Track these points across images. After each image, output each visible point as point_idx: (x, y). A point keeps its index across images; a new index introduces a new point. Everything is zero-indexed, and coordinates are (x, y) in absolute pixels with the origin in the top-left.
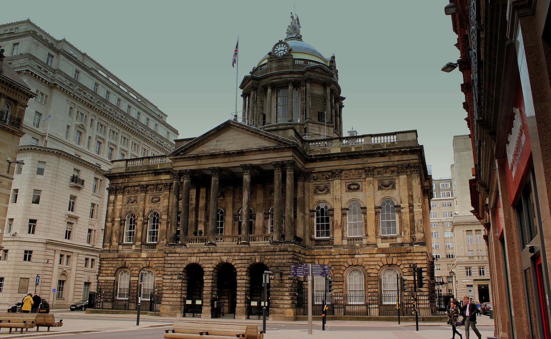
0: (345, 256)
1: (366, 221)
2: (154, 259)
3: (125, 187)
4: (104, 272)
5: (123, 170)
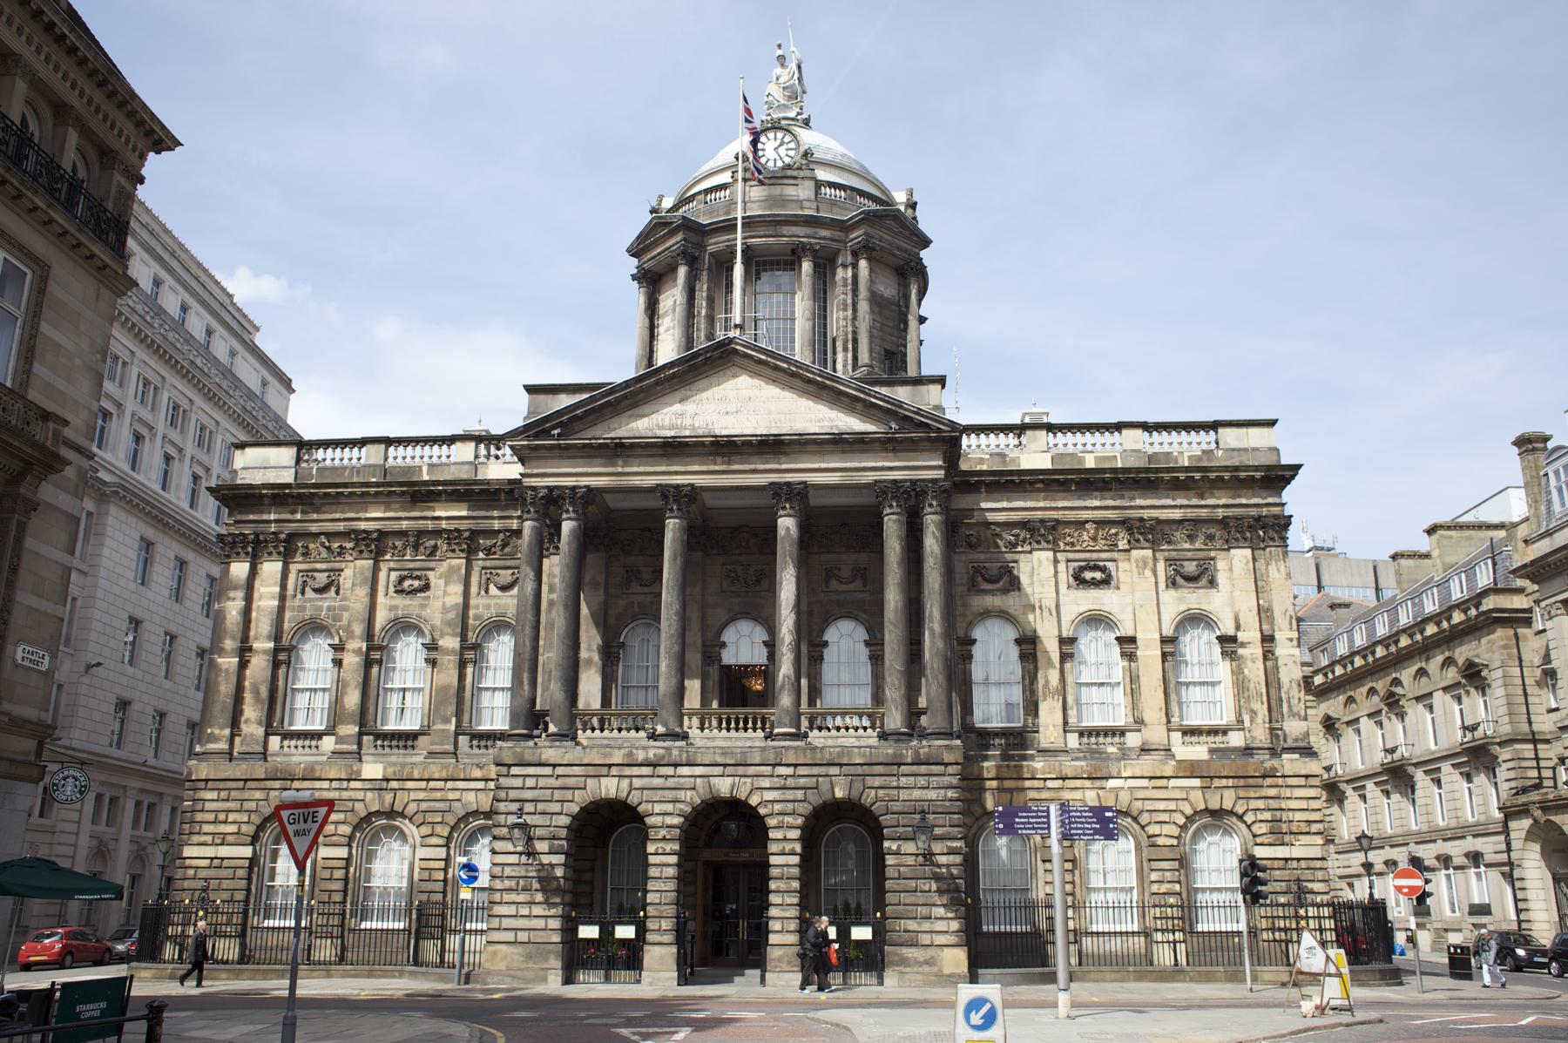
0: (1078, 783)
2: (410, 785)
3: (293, 536)
4: (207, 828)
5: (287, 477)
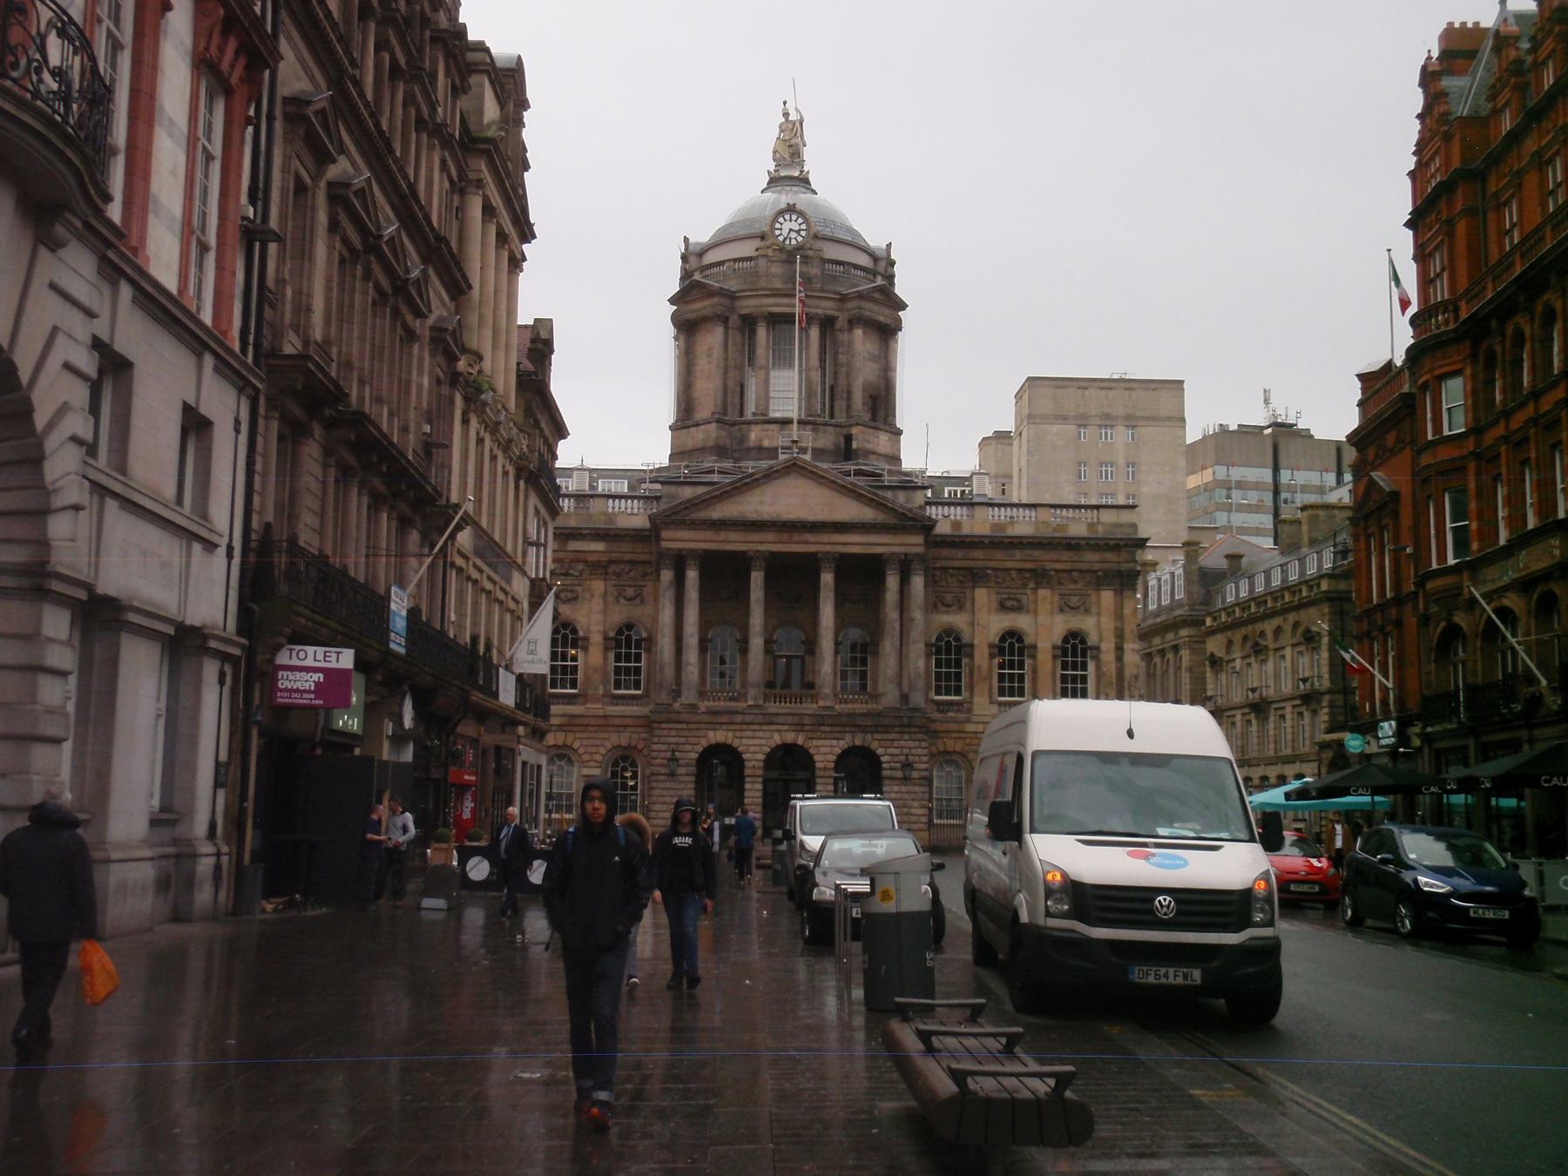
1: (1035, 671)
